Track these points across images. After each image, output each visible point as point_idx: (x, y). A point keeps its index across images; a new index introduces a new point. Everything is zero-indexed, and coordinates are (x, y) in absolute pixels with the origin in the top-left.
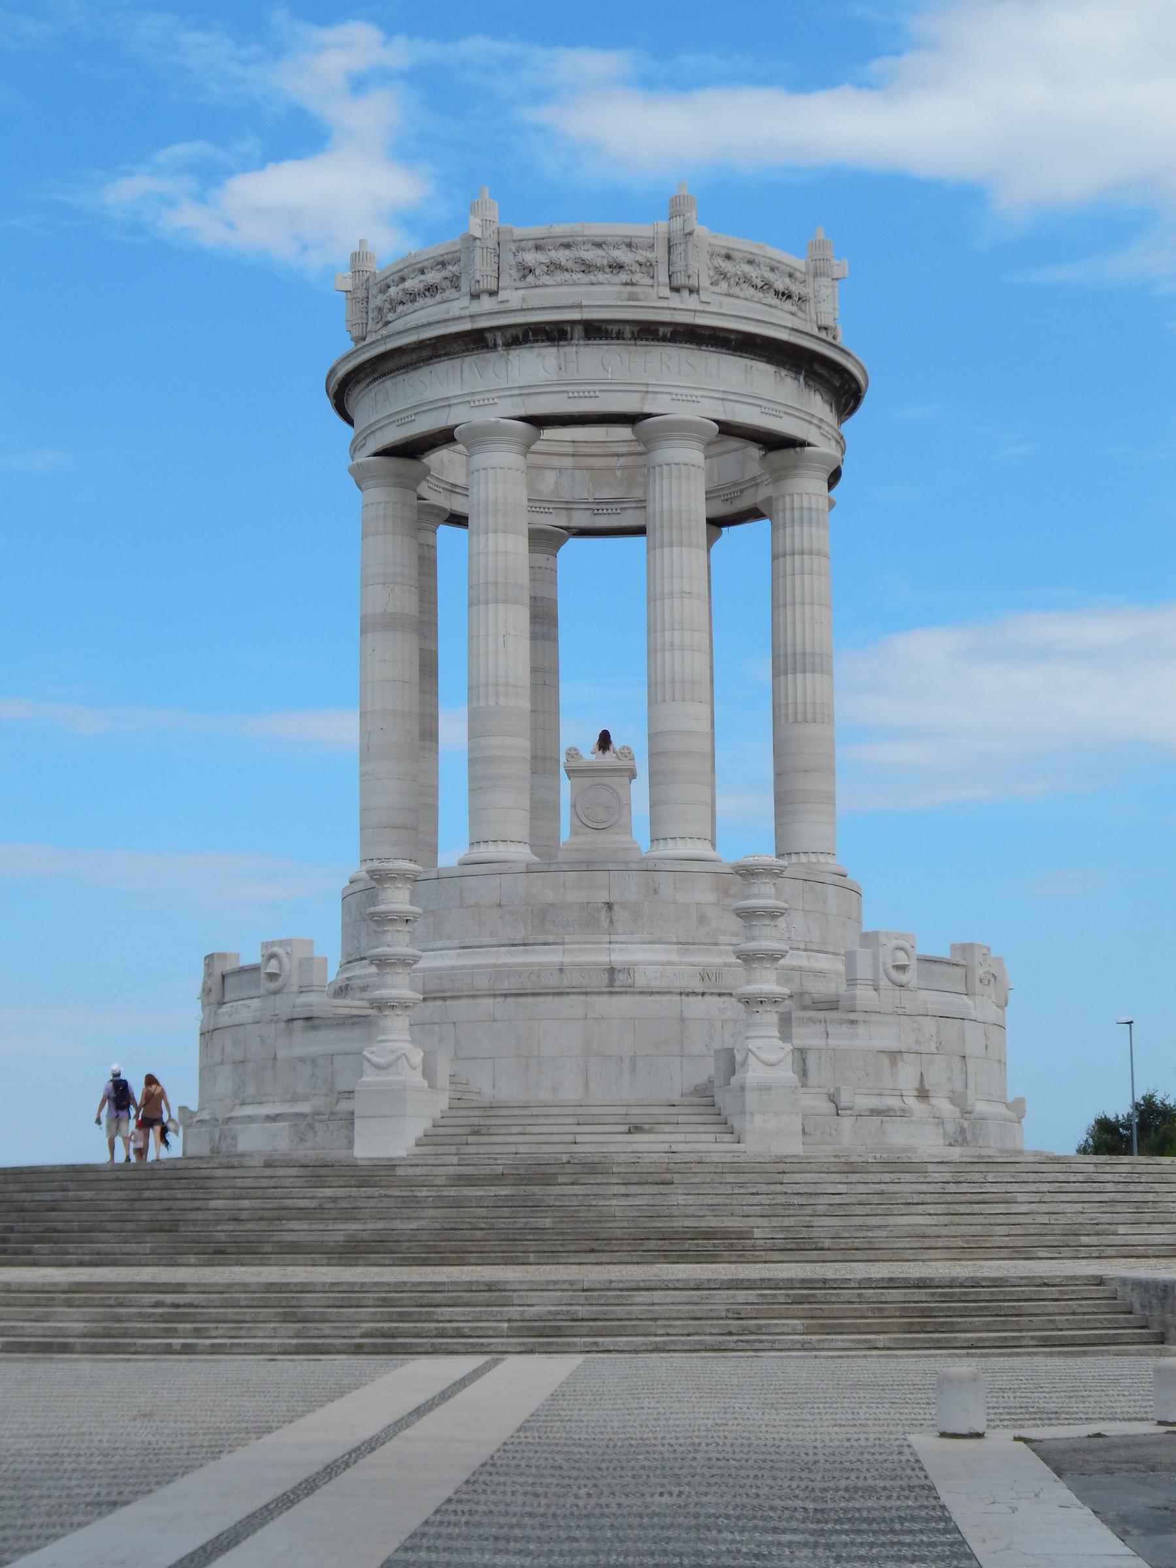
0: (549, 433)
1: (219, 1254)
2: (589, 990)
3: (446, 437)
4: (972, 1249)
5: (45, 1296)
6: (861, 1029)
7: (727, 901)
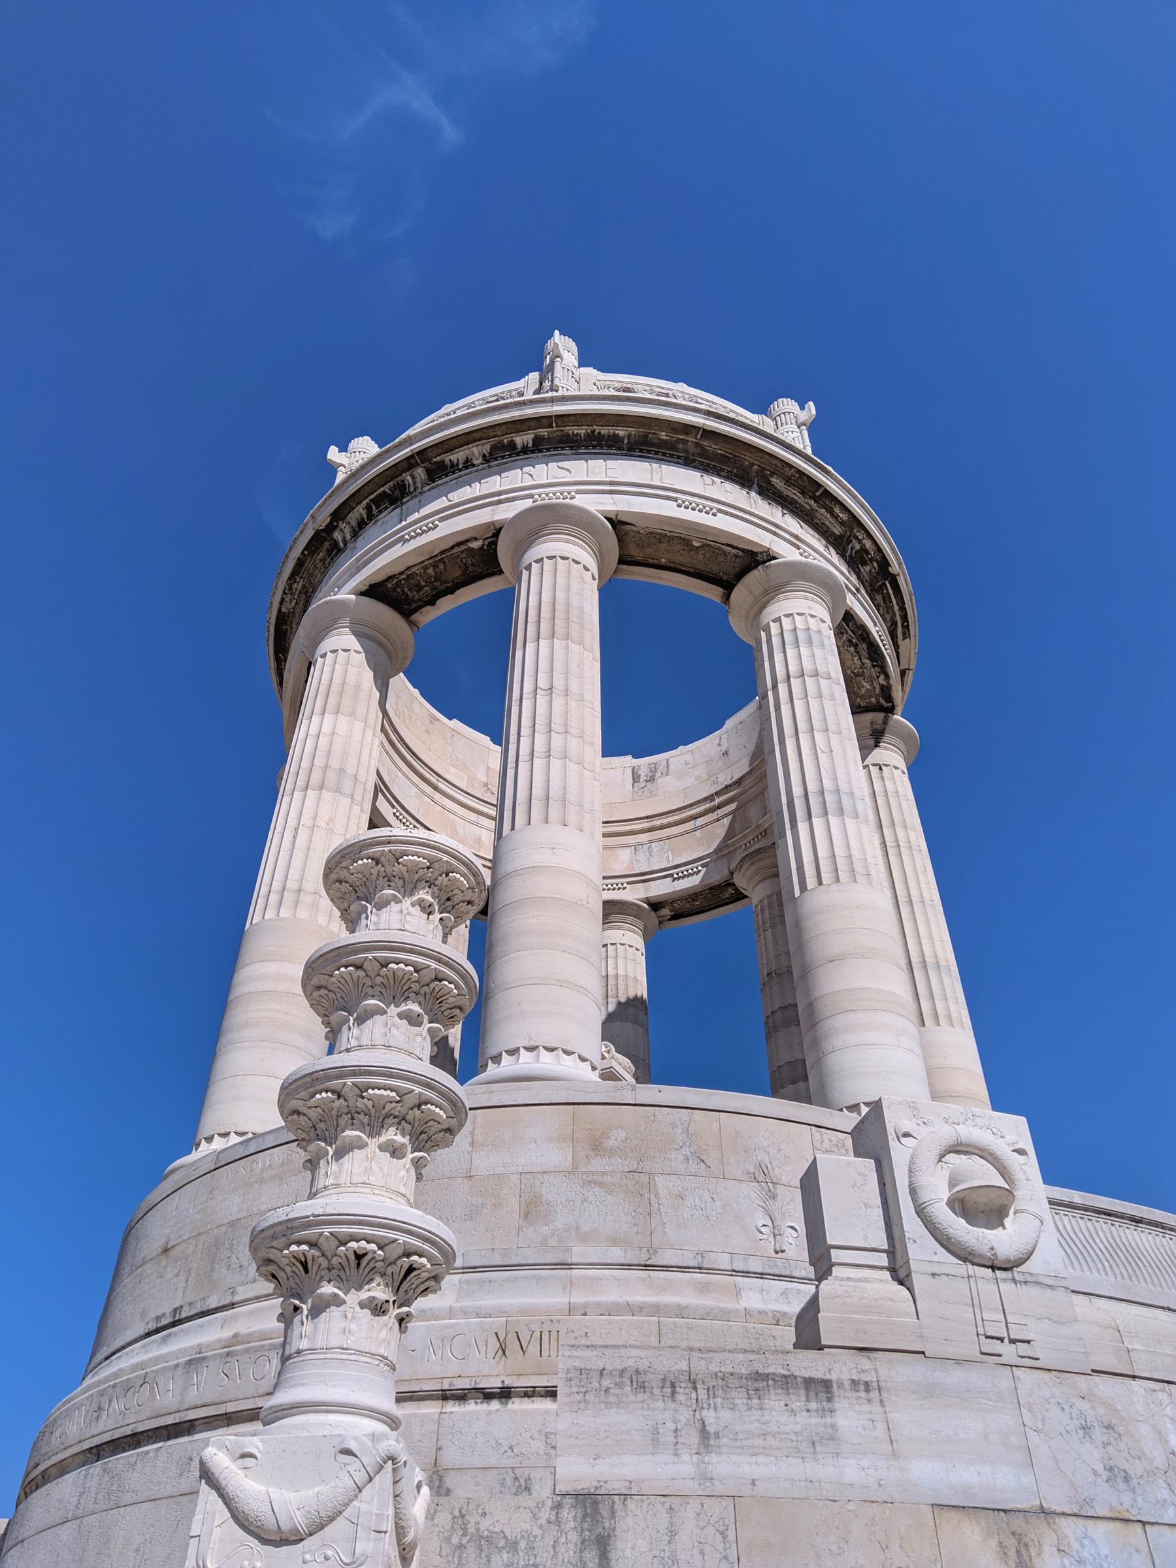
2: (231, 1408)
6: (849, 1416)
7: (598, 1164)
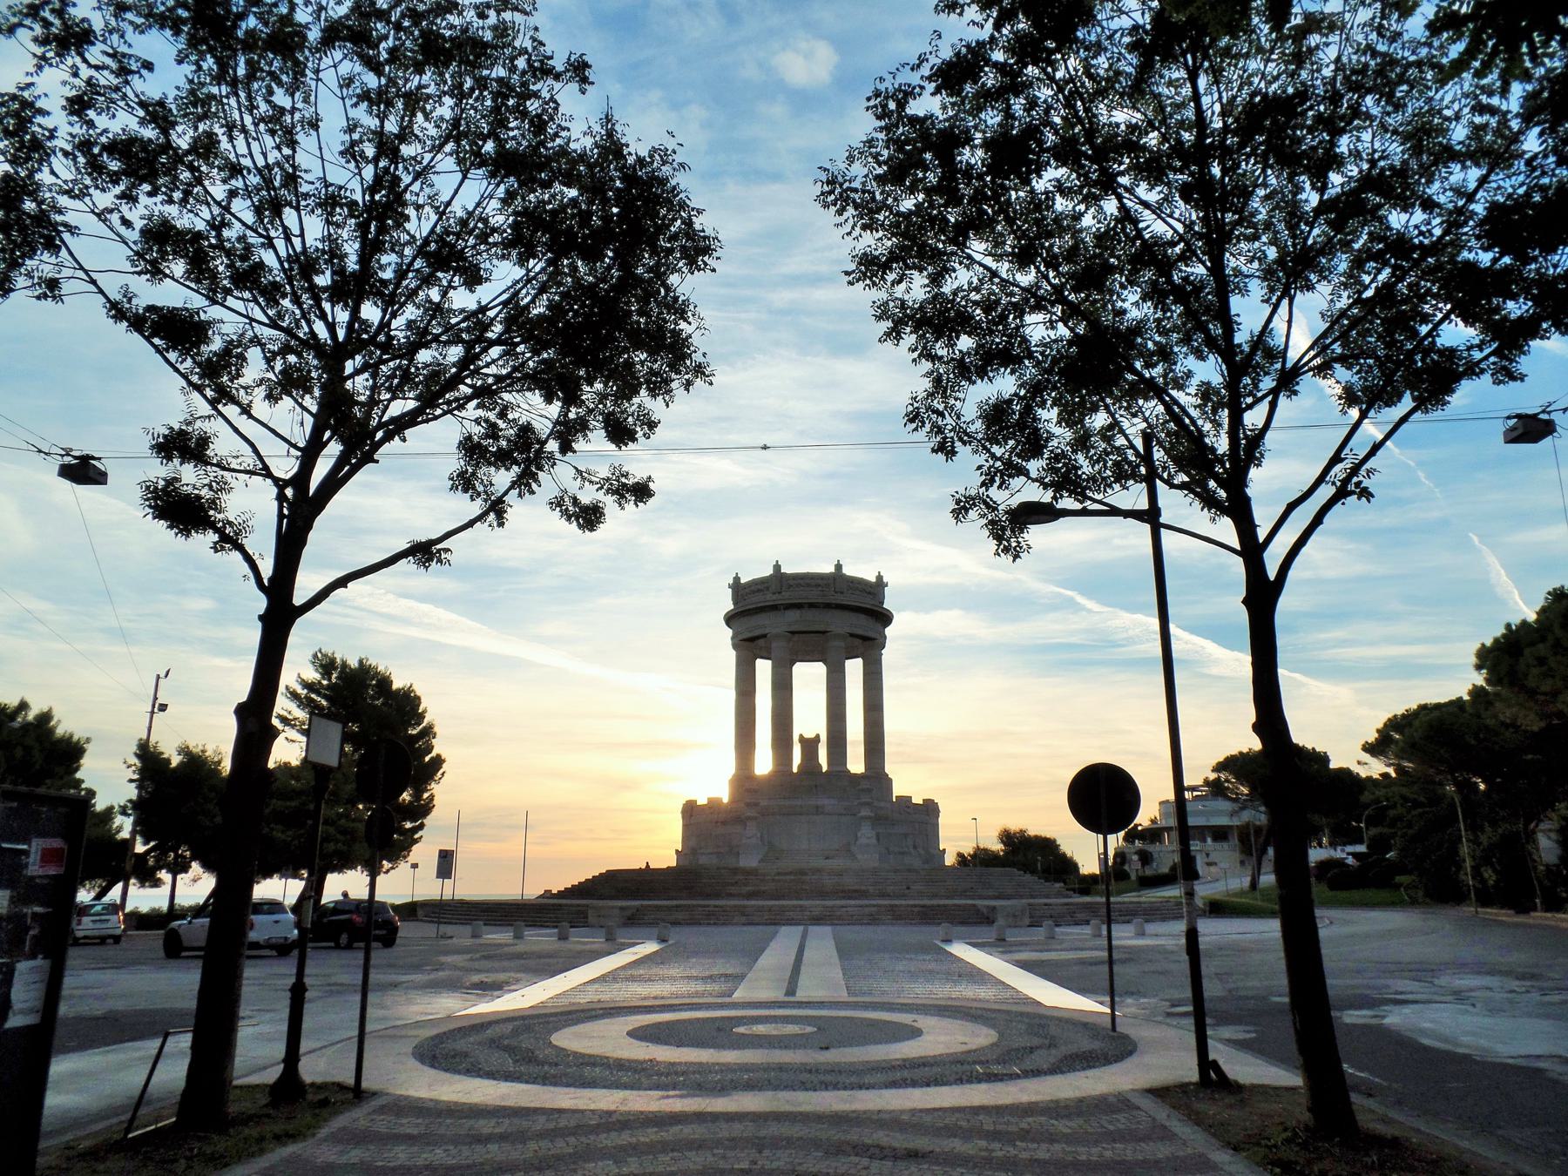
0: (796, 637)
1: (708, 896)
3: (764, 636)
4: (935, 896)
5: (669, 908)
